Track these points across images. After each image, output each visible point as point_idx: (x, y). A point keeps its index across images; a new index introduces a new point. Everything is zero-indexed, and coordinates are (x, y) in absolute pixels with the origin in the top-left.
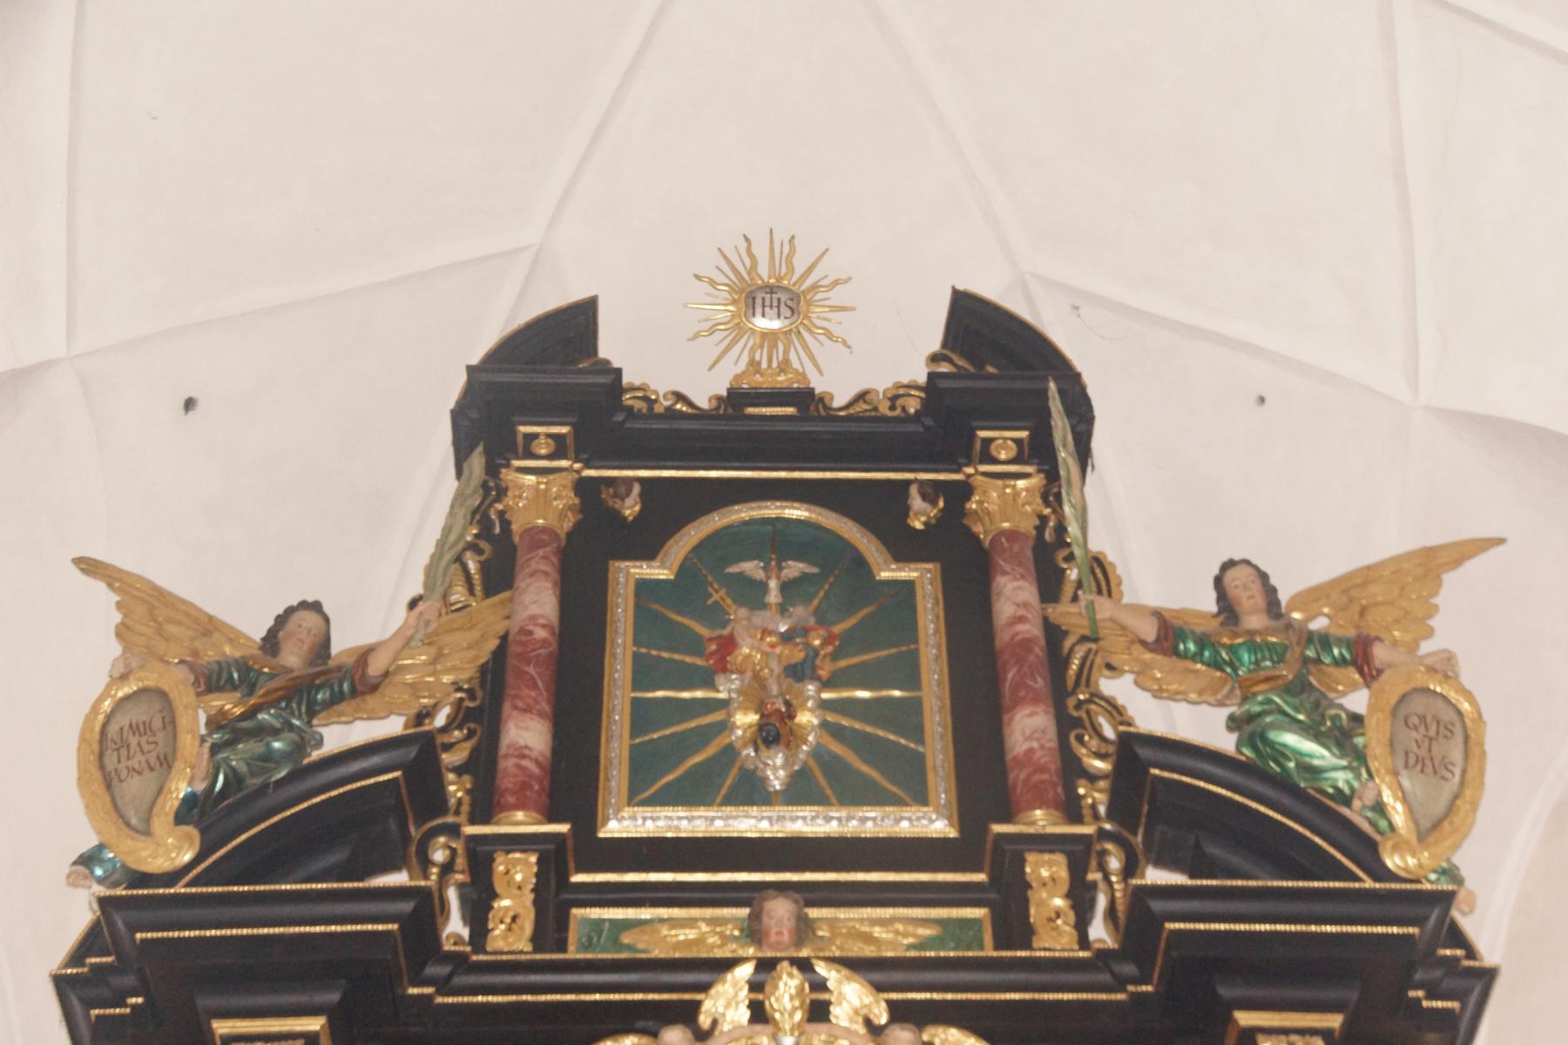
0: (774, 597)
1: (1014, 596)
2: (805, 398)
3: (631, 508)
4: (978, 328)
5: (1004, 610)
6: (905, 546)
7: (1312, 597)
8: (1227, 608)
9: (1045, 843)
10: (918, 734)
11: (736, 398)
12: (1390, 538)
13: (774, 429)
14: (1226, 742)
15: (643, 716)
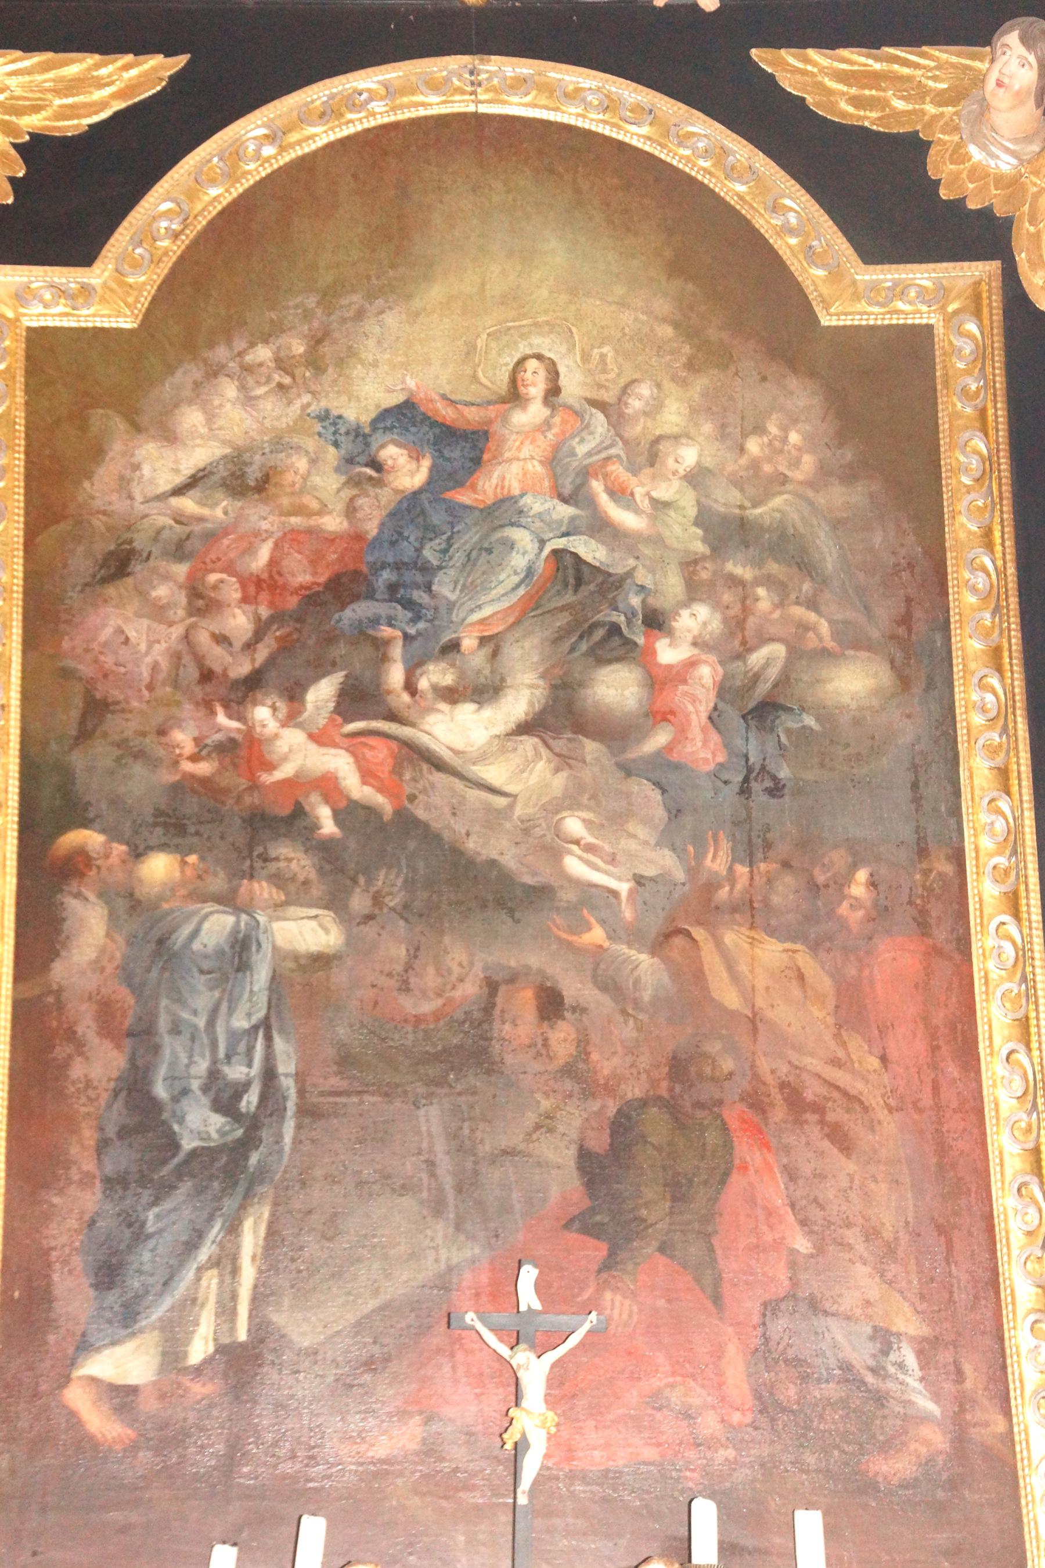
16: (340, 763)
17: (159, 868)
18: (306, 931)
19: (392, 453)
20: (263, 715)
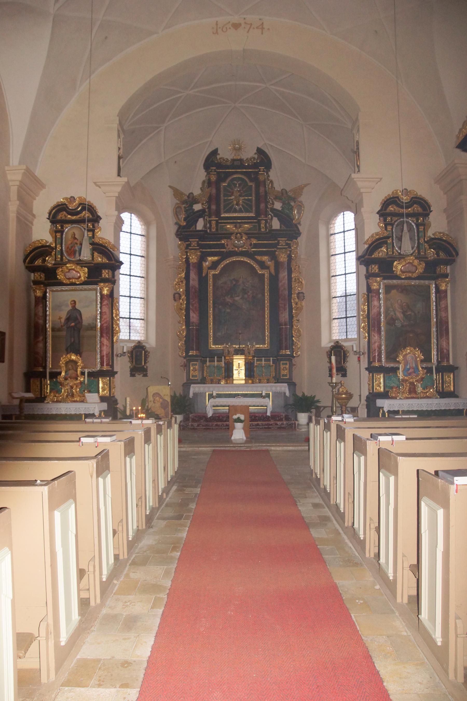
0: (237, 185)
1: (262, 189)
2: (241, 160)
3: (223, 176)
4: (260, 151)
5: (261, 191)
6: (251, 181)
7: (291, 191)
8: (282, 194)
9: (263, 220)
10: (252, 202)
11: (233, 160)
13: (238, 164)
14: (280, 209)
15: (225, 201)
16: (230, 301)
17: (220, 307)
18: (228, 310)
19: (233, 281)
20: (226, 298)
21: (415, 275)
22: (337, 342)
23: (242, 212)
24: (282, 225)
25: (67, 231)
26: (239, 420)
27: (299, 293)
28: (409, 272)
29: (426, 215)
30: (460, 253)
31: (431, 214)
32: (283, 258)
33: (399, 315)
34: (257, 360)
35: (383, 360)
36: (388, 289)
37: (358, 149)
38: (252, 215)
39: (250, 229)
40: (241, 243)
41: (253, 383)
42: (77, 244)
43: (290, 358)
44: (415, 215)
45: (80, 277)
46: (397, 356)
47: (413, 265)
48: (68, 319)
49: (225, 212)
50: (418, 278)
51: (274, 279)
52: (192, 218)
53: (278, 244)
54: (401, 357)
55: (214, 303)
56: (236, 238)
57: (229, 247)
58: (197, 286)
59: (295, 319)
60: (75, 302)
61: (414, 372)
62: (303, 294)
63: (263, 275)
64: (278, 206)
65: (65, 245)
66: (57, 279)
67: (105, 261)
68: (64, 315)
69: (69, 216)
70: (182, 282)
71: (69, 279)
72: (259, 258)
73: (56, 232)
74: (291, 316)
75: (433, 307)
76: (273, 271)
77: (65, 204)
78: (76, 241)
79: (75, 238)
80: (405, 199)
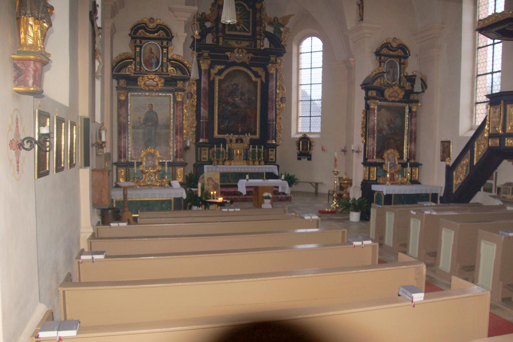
1: (258, 15)
6: (250, 7)
8: (274, 21)
12: (287, 14)
14: (273, 33)
17: (224, 105)
18: (230, 108)
21: (397, 100)
22: (305, 135)
23: (242, 32)
24: (272, 45)
25: (145, 47)
26: (268, 198)
27: (282, 98)
28: (395, 97)
29: (406, 57)
30: (429, 86)
31: (410, 57)
32: (272, 71)
33: (386, 127)
34: (252, 147)
35: (375, 157)
36: (380, 108)
37: (363, 3)
38: (250, 34)
39: (248, 46)
40: (238, 56)
41: (249, 165)
42: (153, 57)
43: (274, 146)
44: (399, 57)
45: (157, 85)
46: (383, 155)
47: (397, 93)
48: (146, 119)
49: (229, 30)
50: (399, 101)
51: (265, 87)
52: (203, 34)
53: (270, 59)
54: (385, 155)
55: (219, 102)
56: (238, 52)
57: (231, 59)
58: (207, 88)
59: (278, 117)
60: (152, 105)
61: (393, 166)
62: (285, 98)
63: (256, 82)
64: (270, 29)
65: (143, 57)
66: (138, 86)
67: (180, 74)
68: (143, 117)
69: (148, 34)
70: (194, 83)
71: (148, 86)
72: (254, 69)
73: (136, 46)
74: (276, 115)
75: (407, 123)
76: (264, 80)
77: (145, 24)
78: (152, 55)
79: (152, 53)
80: (394, 45)
